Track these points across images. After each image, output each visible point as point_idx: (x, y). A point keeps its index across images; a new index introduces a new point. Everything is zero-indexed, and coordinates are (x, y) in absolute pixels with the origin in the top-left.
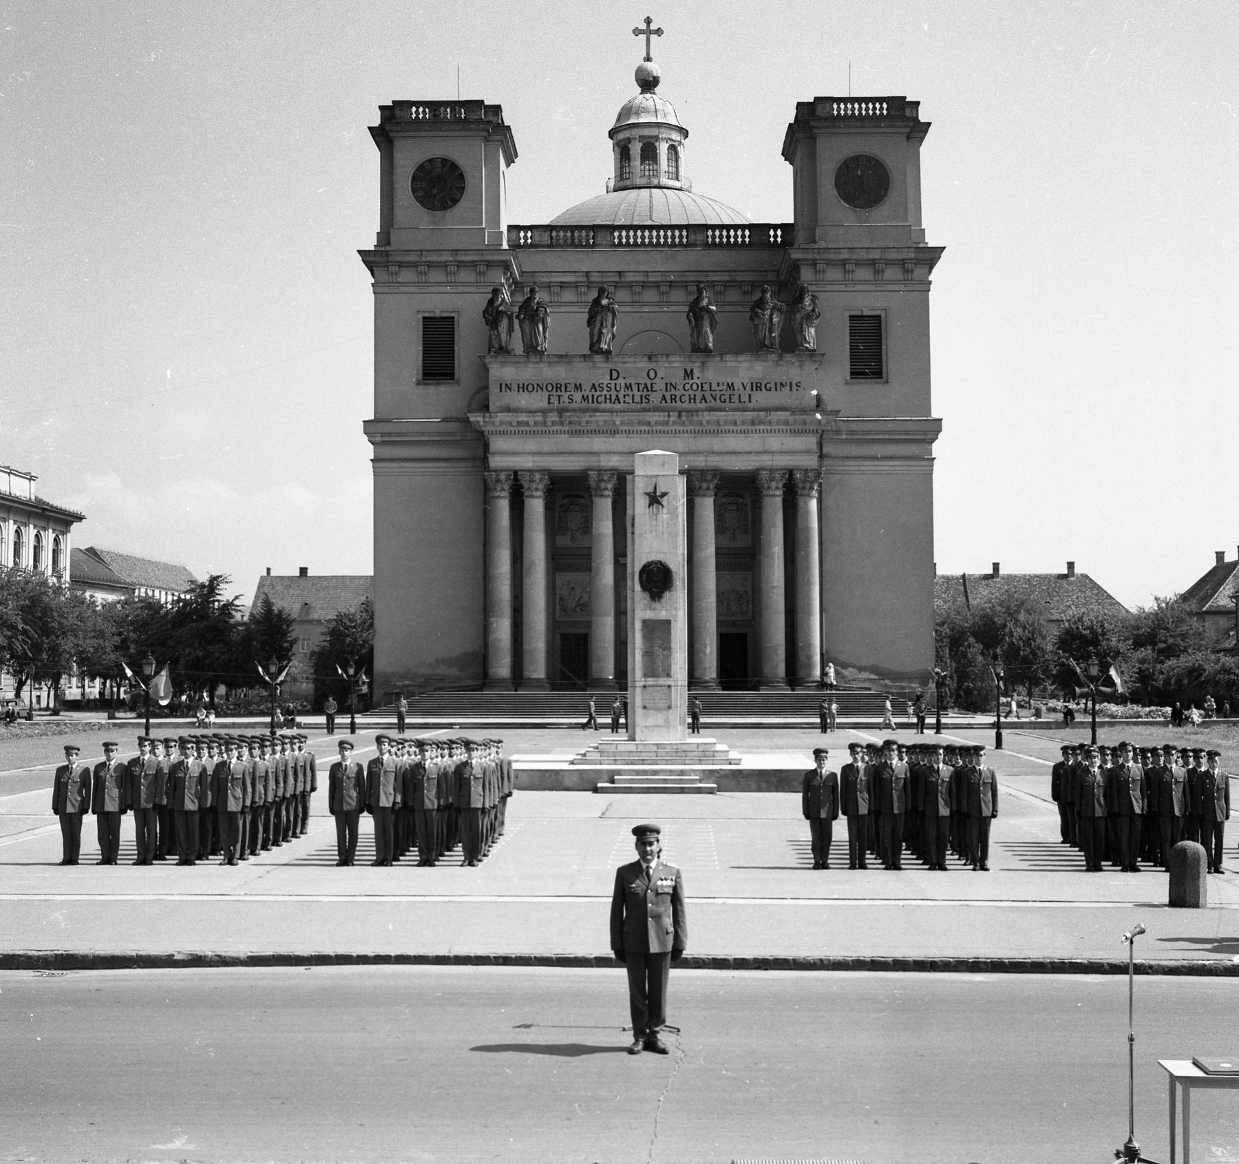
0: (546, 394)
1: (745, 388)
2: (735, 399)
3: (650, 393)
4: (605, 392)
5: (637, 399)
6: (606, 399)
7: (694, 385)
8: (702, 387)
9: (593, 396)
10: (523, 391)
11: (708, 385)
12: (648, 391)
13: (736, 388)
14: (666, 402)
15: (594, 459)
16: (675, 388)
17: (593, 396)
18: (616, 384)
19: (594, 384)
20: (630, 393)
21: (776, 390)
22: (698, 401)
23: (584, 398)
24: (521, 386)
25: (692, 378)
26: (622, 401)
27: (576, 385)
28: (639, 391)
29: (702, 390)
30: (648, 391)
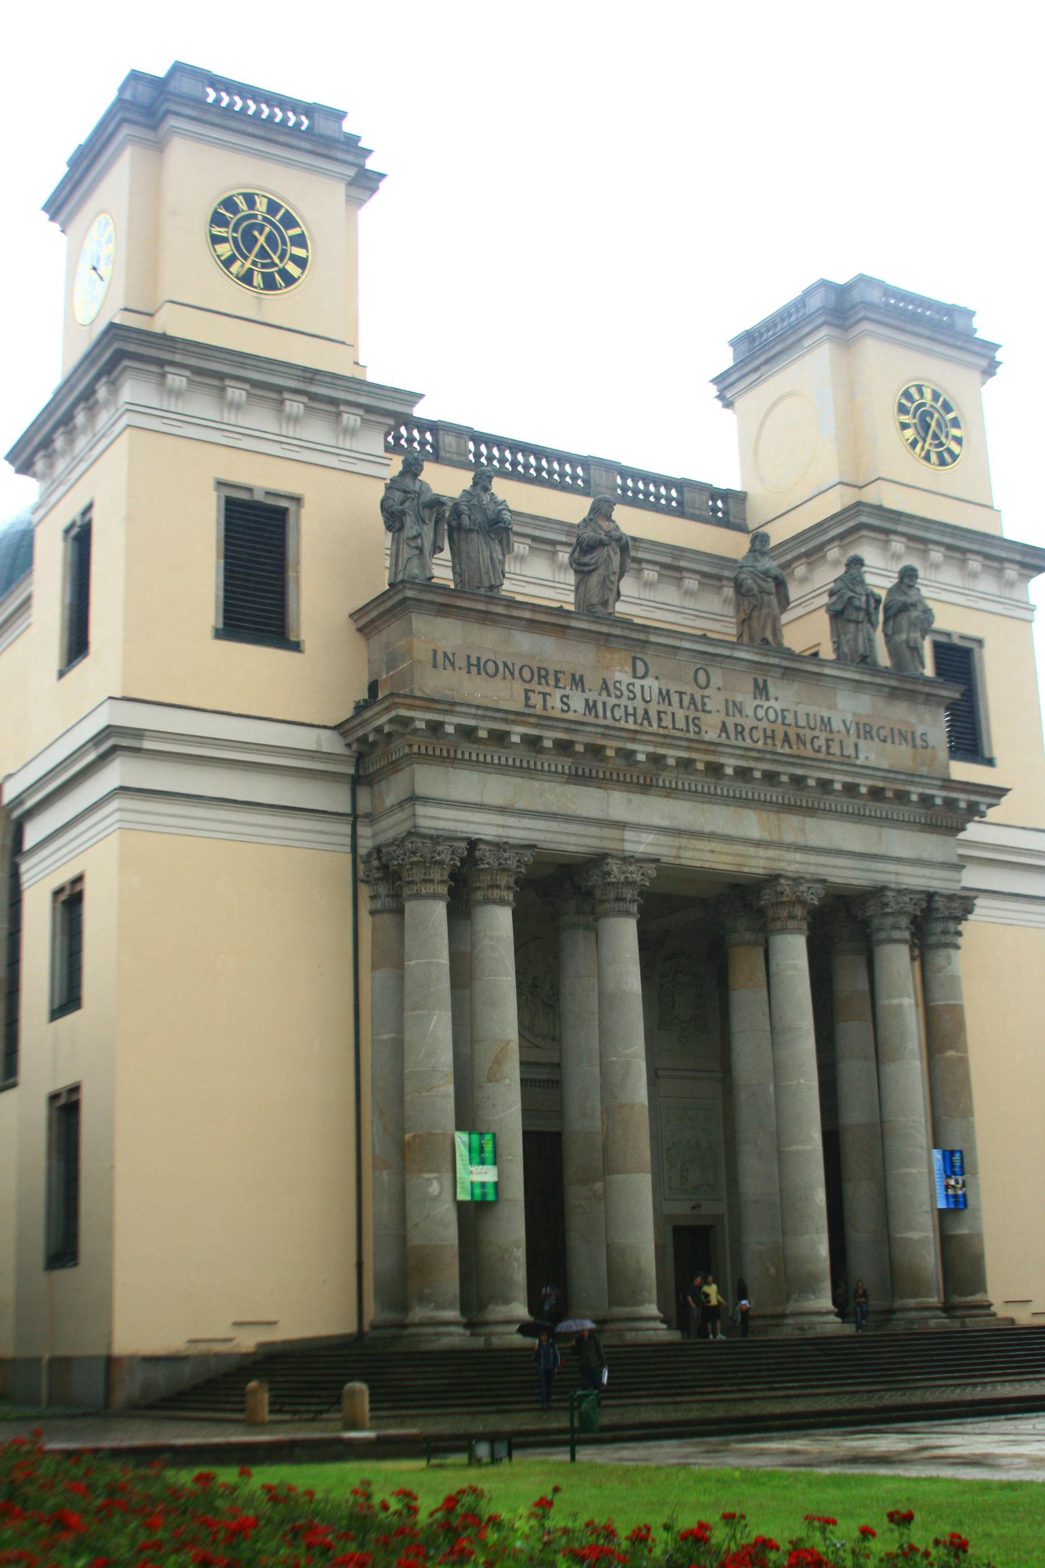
0: (519, 687)
3: (699, 714)
4: (624, 701)
5: (681, 724)
6: (627, 714)
7: (771, 712)
8: (784, 718)
9: (604, 704)
10: (479, 673)
13: (835, 728)
15: (615, 833)
16: (740, 712)
17: (604, 704)
18: (642, 687)
19: (605, 682)
20: (669, 710)
21: (893, 742)
22: (778, 743)
23: (591, 707)
24: (474, 661)
25: (767, 699)
27: (573, 675)
28: (681, 706)
29: (783, 724)
30: (697, 710)
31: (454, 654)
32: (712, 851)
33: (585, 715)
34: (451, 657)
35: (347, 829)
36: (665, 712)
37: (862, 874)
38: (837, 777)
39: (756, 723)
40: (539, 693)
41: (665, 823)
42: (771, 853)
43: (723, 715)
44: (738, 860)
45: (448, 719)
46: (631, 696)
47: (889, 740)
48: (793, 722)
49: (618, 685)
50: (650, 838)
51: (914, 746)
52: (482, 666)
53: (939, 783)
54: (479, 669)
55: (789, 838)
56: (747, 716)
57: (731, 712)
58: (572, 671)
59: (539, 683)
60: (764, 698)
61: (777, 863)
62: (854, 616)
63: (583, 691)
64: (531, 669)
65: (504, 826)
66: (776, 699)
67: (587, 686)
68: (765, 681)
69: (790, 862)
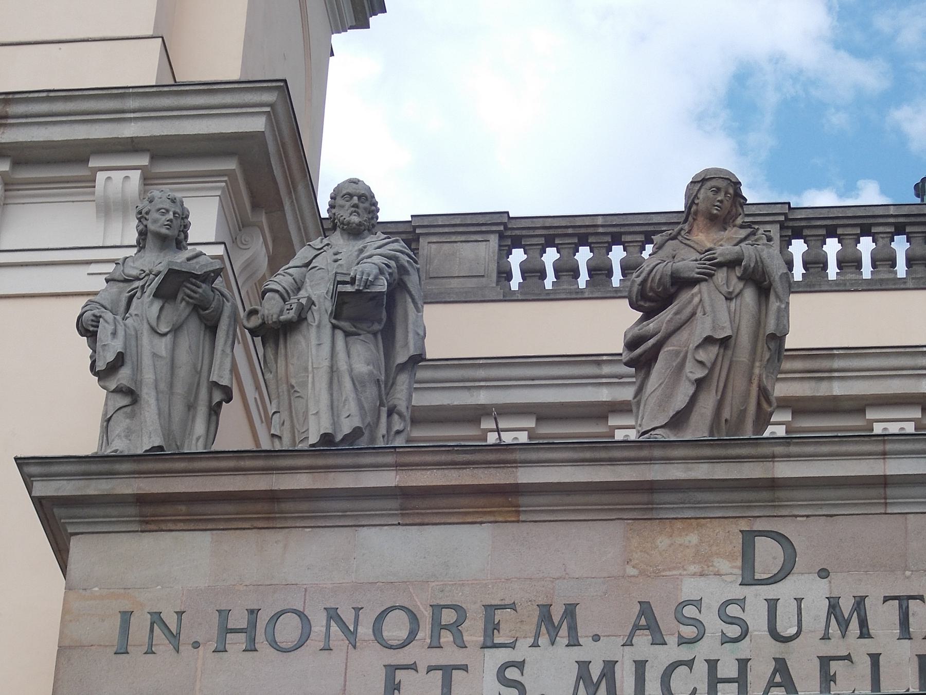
9: (640, 666)
17: (640, 666)
18: (772, 605)
19: (646, 609)
20: (861, 649)
24: (238, 620)
27: (545, 613)
31: (180, 614)
34: (172, 622)
36: (848, 658)
40: (430, 669)
46: (734, 631)
49: (689, 611)
54: (252, 640)
58: (542, 600)
59: (436, 645)
63: (574, 642)
64: (414, 618)
67: (583, 631)
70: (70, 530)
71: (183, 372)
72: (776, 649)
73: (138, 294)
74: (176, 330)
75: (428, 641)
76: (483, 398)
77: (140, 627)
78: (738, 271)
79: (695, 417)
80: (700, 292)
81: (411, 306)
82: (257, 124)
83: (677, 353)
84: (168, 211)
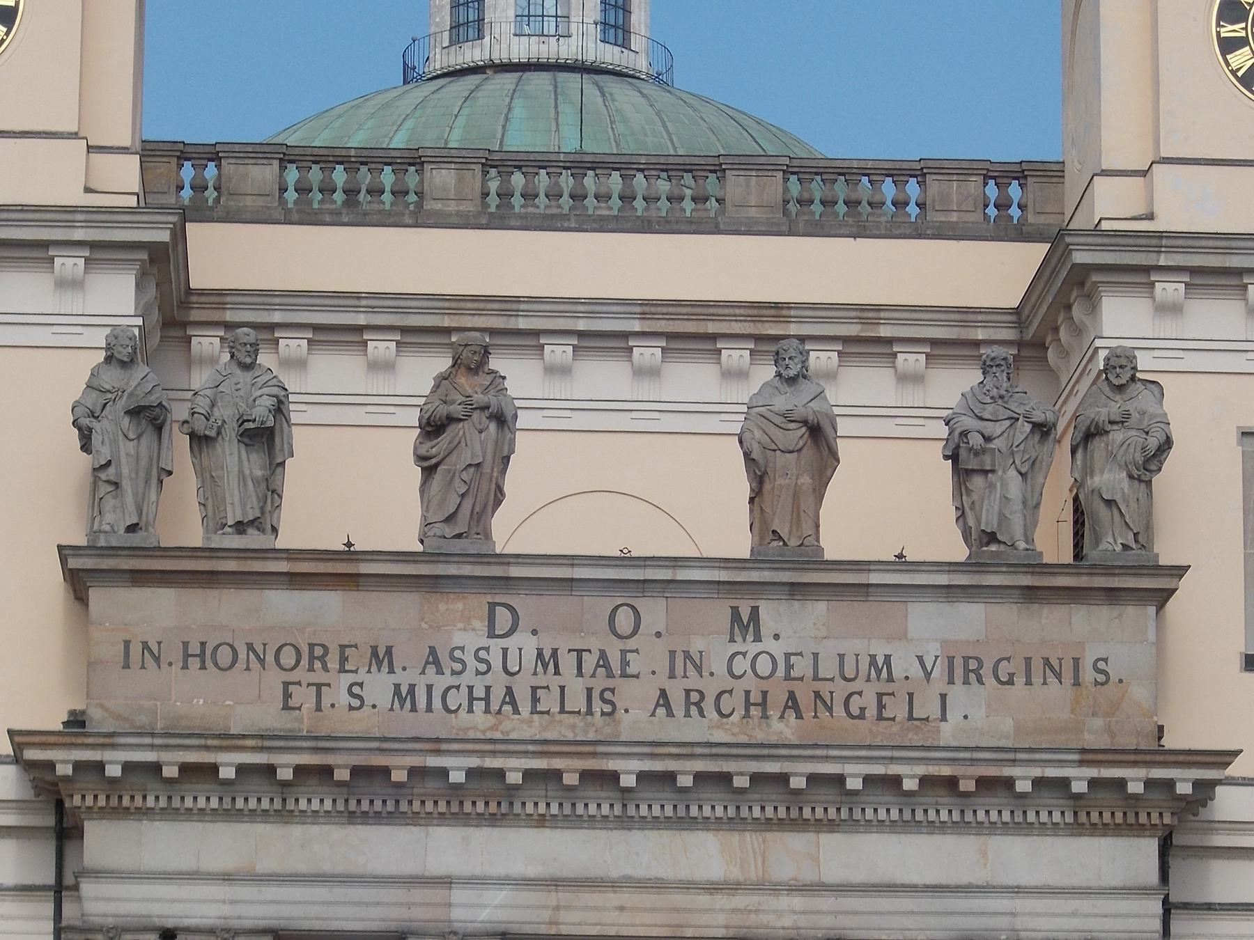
0: (274, 679)
1: (928, 675)
2: (896, 709)
3: (616, 682)
4: (468, 678)
5: (576, 701)
6: (471, 699)
8: (789, 667)
9: (430, 688)
10: (203, 667)
11: (810, 660)
12: (610, 675)
14: (670, 713)
15: (437, 894)
16: (699, 669)
17: (430, 688)
18: (505, 651)
19: (433, 651)
21: (1029, 683)
22: (774, 713)
23: (404, 696)
24: (194, 648)
25: (758, 638)
26: (525, 709)
28: (580, 673)
29: (788, 677)
30: (610, 675)
31: (159, 643)
32: (622, 909)
33: (392, 709)
35: (49, 908)
36: (547, 687)
37: (932, 921)
38: (849, 769)
39: (729, 683)
40: (309, 685)
41: (532, 871)
42: (741, 901)
43: (662, 680)
44: (674, 918)
45: (108, 755)
46: (483, 667)
47: (1020, 680)
48: (810, 673)
49: (457, 654)
50: (499, 896)
51: (1077, 684)
52: (208, 653)
53: (1076, 757)
54: (203, 662)
55: (784, 871)
56: (712, 674)
57: (679, 671)
59: (311, 669)
60: (750, 638)
61: (752, 916)
62: (973, 464)
63: (391, 671)
64: (298, 652)
65: (232, 902)
66: (777, 637)
68: (755, 610)
69: (779, 914)
70: (88, 584)
71: (144, 462)
72: (504, 680)
73: (111, 403)
74: (139, 437)
75: (307, 667)
76: (277, 317)
77: (136, 649)
78: (487, 413)
79: (460, 516)
80: (463, 426)
81: (285, 424)
82: (164, 236)
83: (449, 471)
84: (128, 346)
